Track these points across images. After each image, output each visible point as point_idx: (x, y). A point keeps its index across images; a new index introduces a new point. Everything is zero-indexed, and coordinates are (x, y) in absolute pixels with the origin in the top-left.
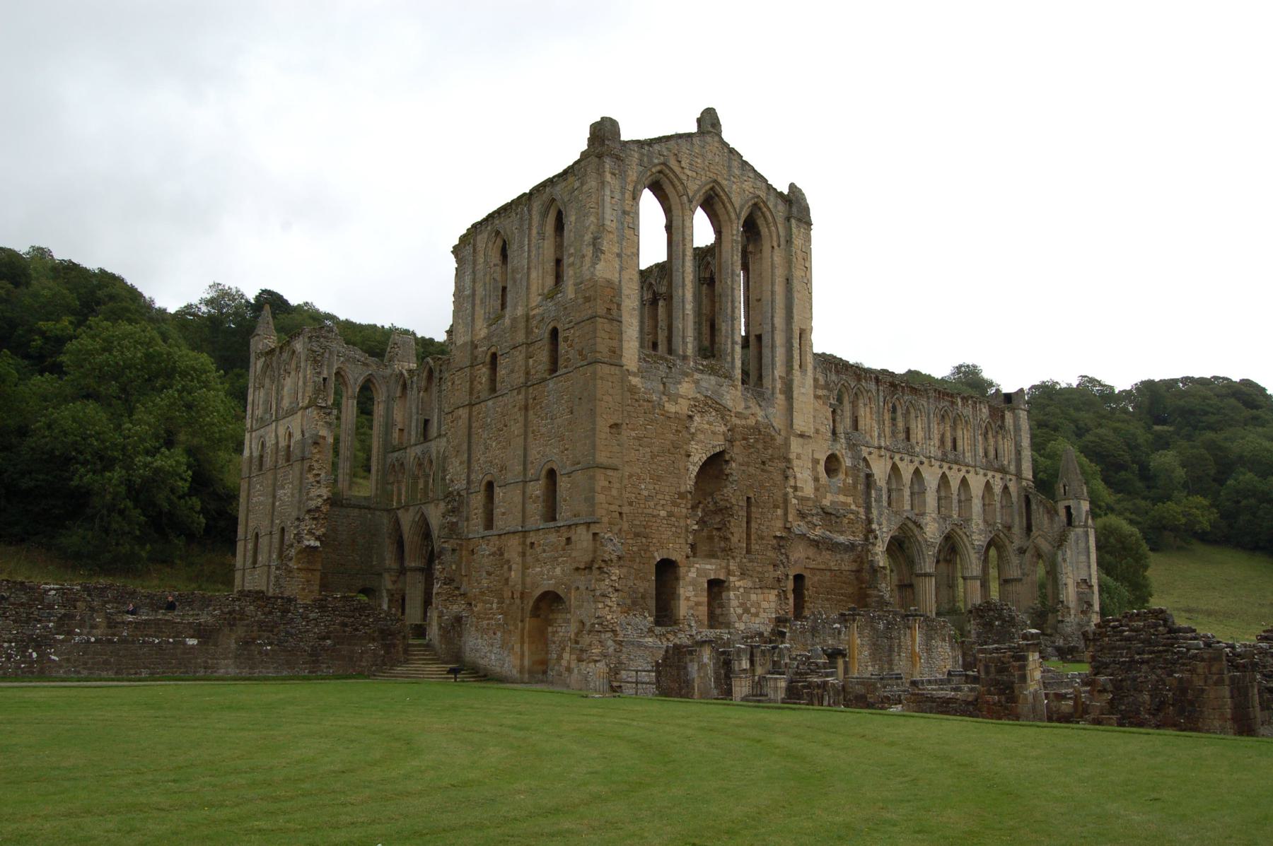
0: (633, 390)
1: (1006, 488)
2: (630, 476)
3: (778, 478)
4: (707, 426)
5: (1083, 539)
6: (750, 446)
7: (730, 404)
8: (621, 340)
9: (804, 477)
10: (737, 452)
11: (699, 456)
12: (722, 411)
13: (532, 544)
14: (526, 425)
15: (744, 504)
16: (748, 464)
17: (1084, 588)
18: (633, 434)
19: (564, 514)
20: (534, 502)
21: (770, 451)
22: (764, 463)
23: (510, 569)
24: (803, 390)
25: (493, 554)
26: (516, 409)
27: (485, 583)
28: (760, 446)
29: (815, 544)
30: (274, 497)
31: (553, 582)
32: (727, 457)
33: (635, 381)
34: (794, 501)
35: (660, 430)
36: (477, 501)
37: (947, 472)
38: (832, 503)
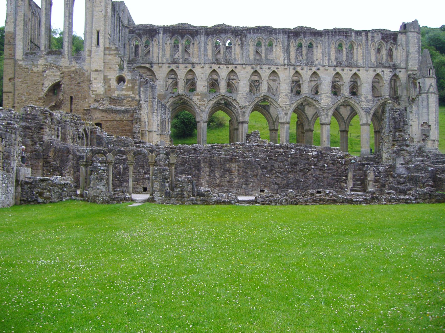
0: (20, 66)
1: (395, 75)
2: (19, 94)
3: (86, 88)
4: (51, 73)
5: (426, 100)
6: (73, 78)
7: (61, 64)
8: (15, 51)
9: (98, 87)
10: (65, 82)
11: (48, 84)
12: (59, 68)
15: (69, 99)
16: (71, 85)
17: (425, 127)
18: (20, 80)
21: (82, 79)
22: (79, 83)
24: (97, 54)
28: (77, 77)
29: (106, 111)
32: (61, 83)
33: (20, 63)
34: (92, 96)
35: (31, 77)
37: (340, 72)
38: (118, 95)
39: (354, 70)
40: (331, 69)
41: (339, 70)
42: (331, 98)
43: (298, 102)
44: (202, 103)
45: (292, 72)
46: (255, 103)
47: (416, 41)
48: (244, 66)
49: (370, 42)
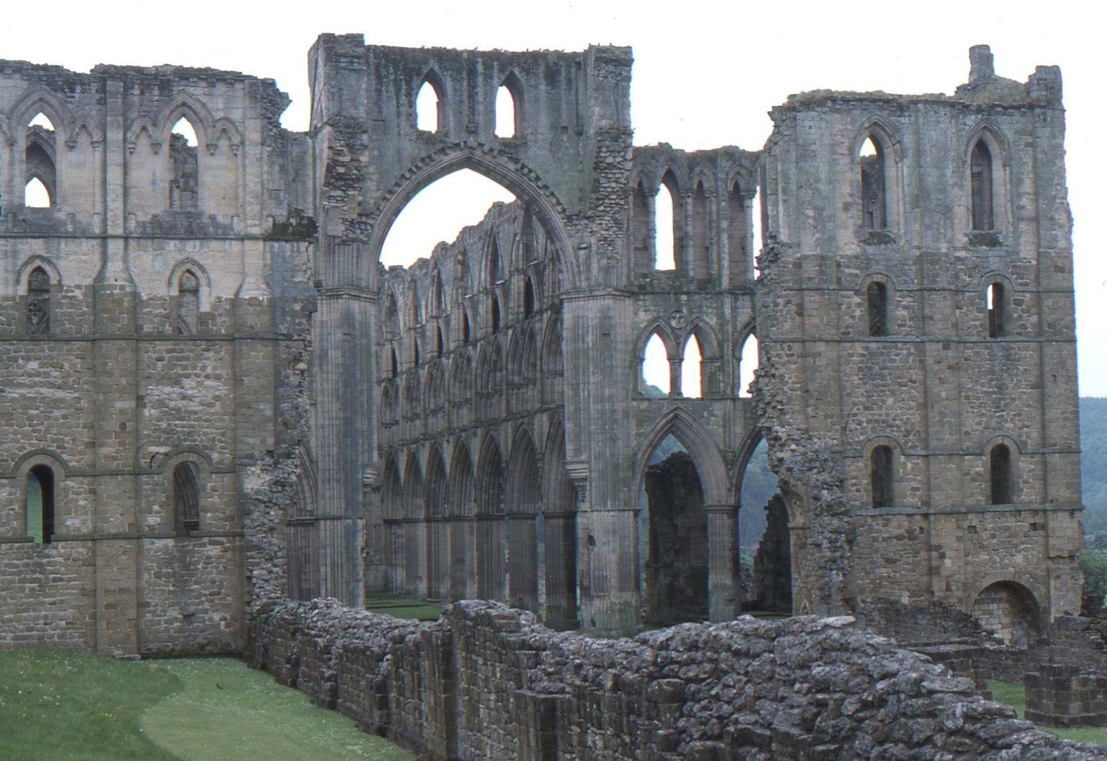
13: (972, 529)
14: (960, 387)
19: (1028, 494)
20: (973, 480)
23: (942, 556)
25: (900, 538)
26: (943, 366)
27: (883, 572)
30: (140, 400)
31: (1012, 570)
36: (859, 471)
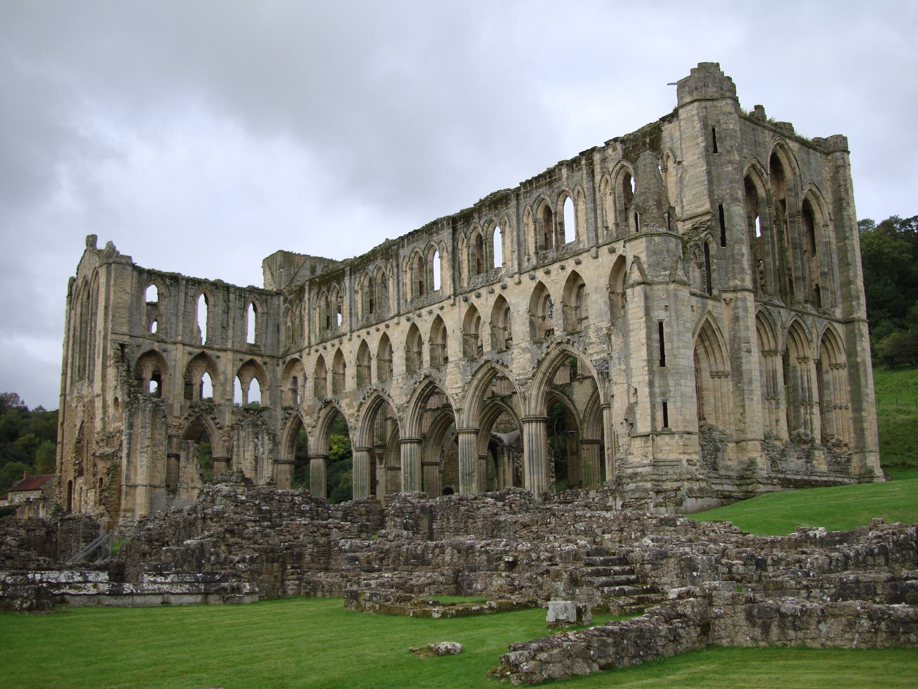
39: (570, 265)
40: (525, 278)
41: (540, 275)
42: (530, 351)
43: (479, 376)
44: (352, 411)
45: (464, 308)
46: (417, 394)
47: (698, 126)
48: (396, 320)
49: (598, 178)
